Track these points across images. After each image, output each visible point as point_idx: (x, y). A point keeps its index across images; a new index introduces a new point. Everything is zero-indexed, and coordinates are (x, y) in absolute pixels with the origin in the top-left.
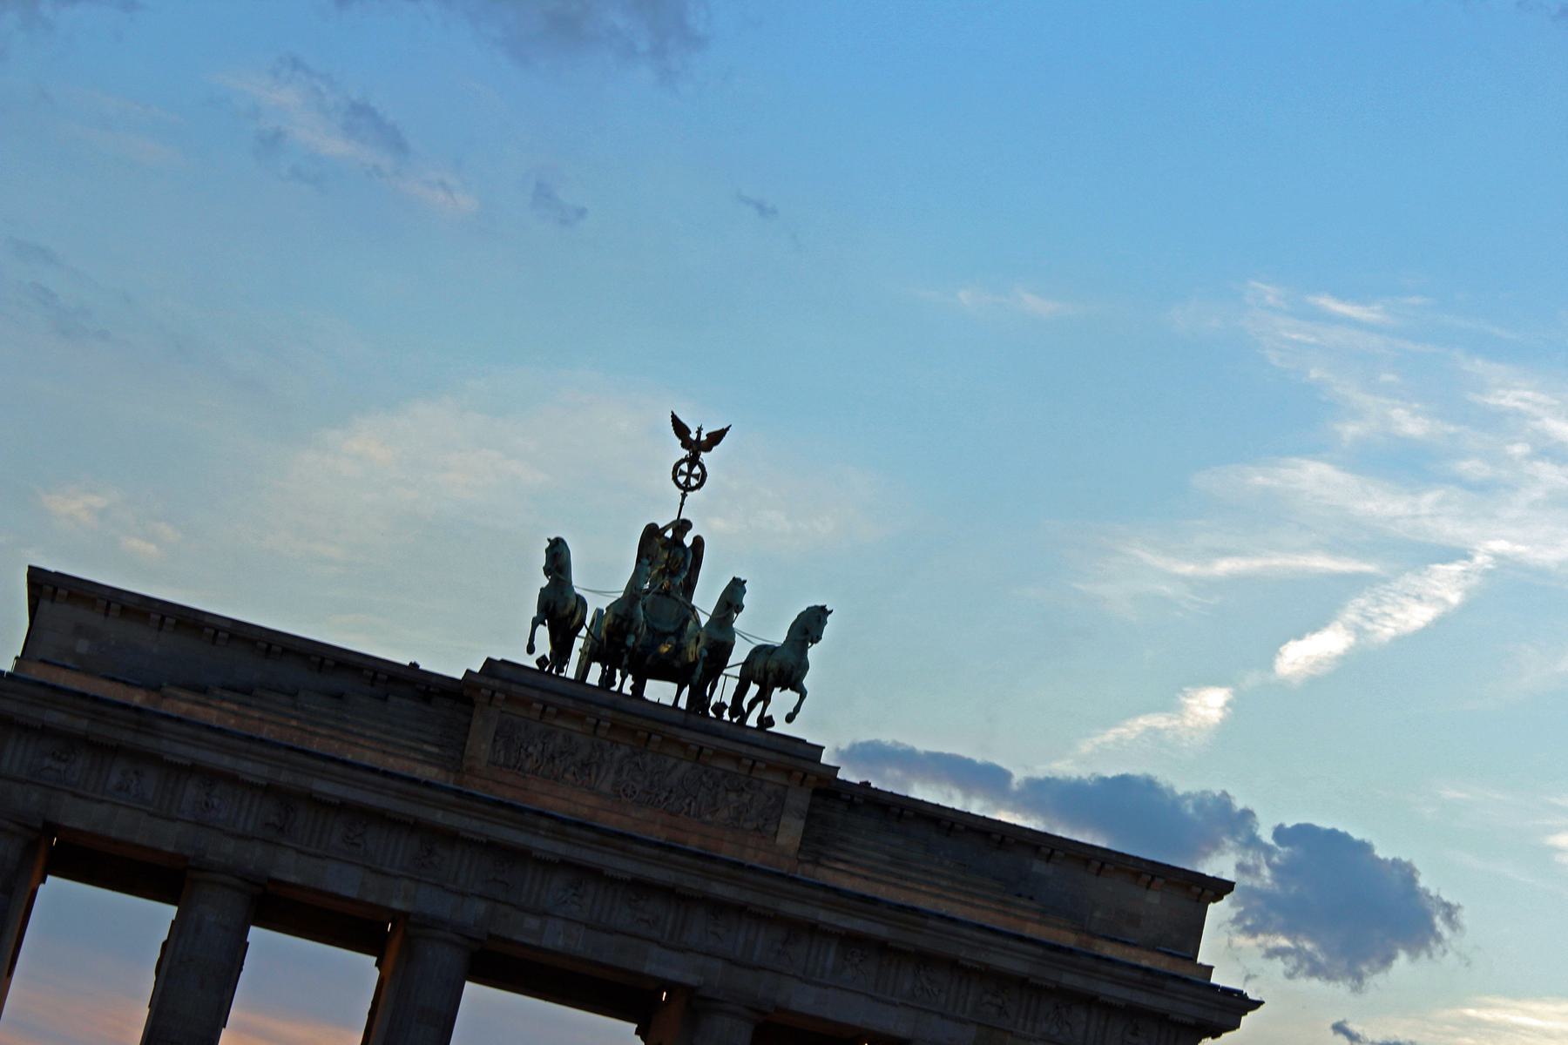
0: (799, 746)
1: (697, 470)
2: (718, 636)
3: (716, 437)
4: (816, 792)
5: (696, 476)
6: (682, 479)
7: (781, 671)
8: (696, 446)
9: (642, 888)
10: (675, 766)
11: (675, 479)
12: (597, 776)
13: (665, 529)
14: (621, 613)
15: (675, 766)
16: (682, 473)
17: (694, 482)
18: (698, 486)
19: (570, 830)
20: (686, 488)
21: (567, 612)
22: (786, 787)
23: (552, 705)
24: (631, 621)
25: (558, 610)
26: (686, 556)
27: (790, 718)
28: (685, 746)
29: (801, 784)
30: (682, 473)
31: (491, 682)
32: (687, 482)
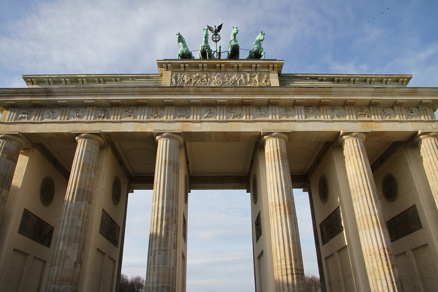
2: (235, 44)
3: (220, 27)
6: (214, 39)
9: (231, 106)
11: (213, 39)
12: (207, 81)
17: (218, 39)
18: (219, 40)
19: (200, 89)
20: (216, 41)
21: (188, 53)
22: (269, 72)
28: (233, 67)
29: (273, 70)
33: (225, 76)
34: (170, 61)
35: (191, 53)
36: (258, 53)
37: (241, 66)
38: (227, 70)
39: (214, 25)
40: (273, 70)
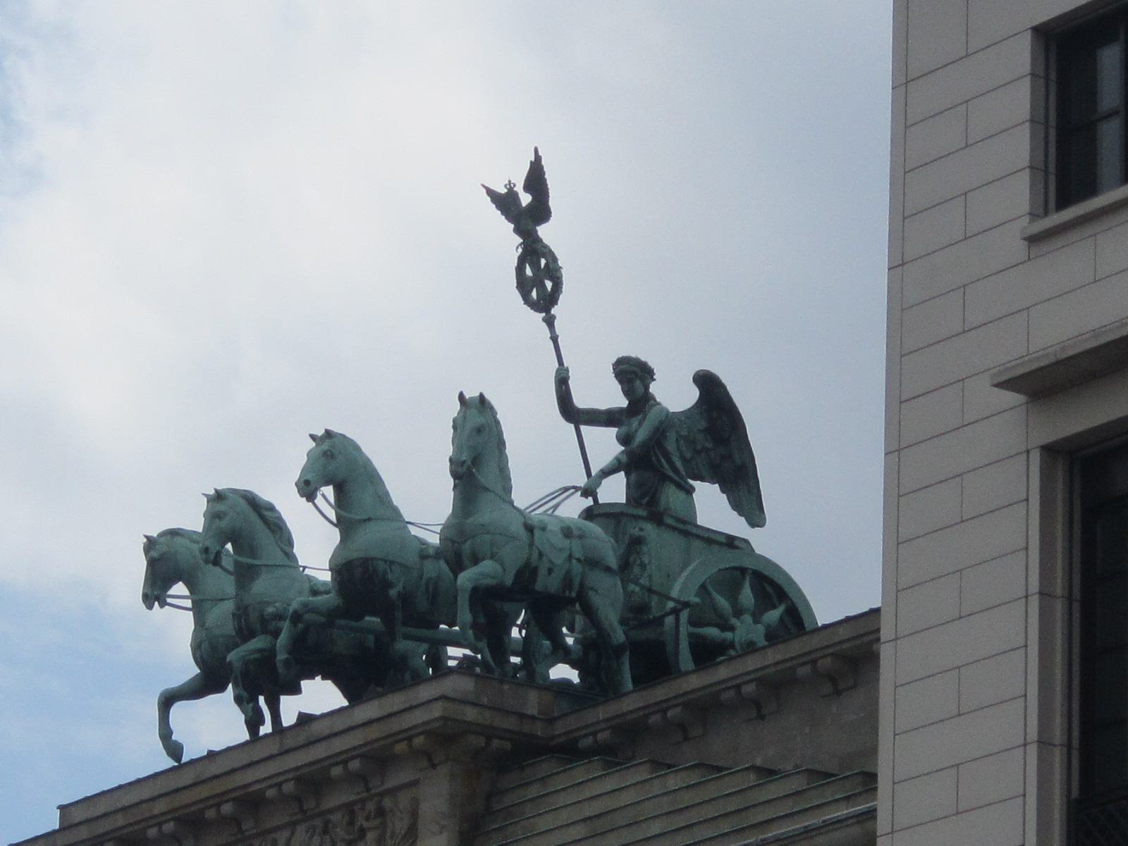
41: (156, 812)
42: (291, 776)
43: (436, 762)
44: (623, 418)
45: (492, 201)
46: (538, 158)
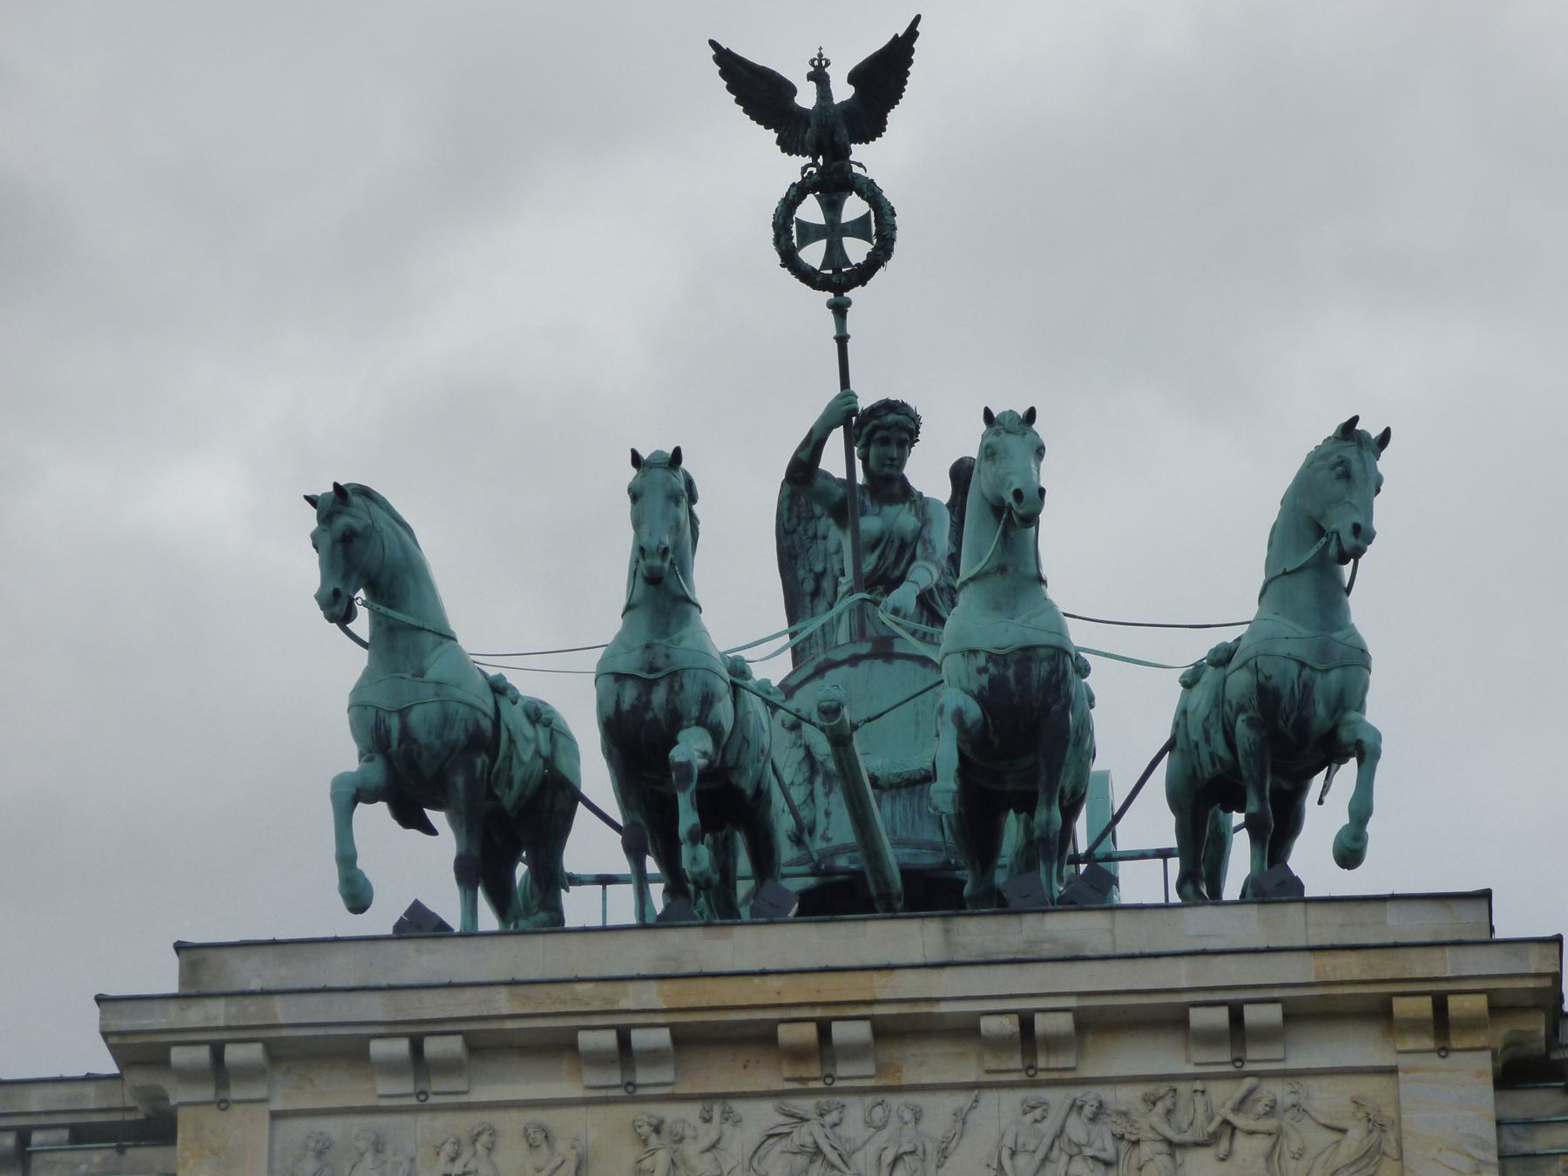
0: (1392, 913)
1: (854, 208)
2: (1005, 633)
3: (885, 75)
4: (1514, 1073)
5: (859, 228)
6: (814, 254)
7: (1266, 696)
8: (828, 127)
10: (961, 1118)
11: (789, 259)
13: (814, 445)
14: (628, 663)
15: (961, 1118)
16: (809, 233)
17: (857, 250)
20: (839, 281)
21: (458, 734)
22: (1392, 1071)
23: (442, 1028)
24: (674, 675)
25: (448, 761)
26: (925, 522)
27: (1349, 854)
30: (809, 233)
31: (196, 1015)
32: (835, 254)
33: (888, 1157)
34: (252, 1012)
35: (498, 688)
36: (1303, 724)
37: (1055, 1043)
38: (909, 1078)
39: (811, 45)
40: (1444, 1051)
41: (625, 1004)
42: (1072, 1002)
43: (1454, 1044)
44: (868, 503)
45: (722, 74)
46: (912, 33)
